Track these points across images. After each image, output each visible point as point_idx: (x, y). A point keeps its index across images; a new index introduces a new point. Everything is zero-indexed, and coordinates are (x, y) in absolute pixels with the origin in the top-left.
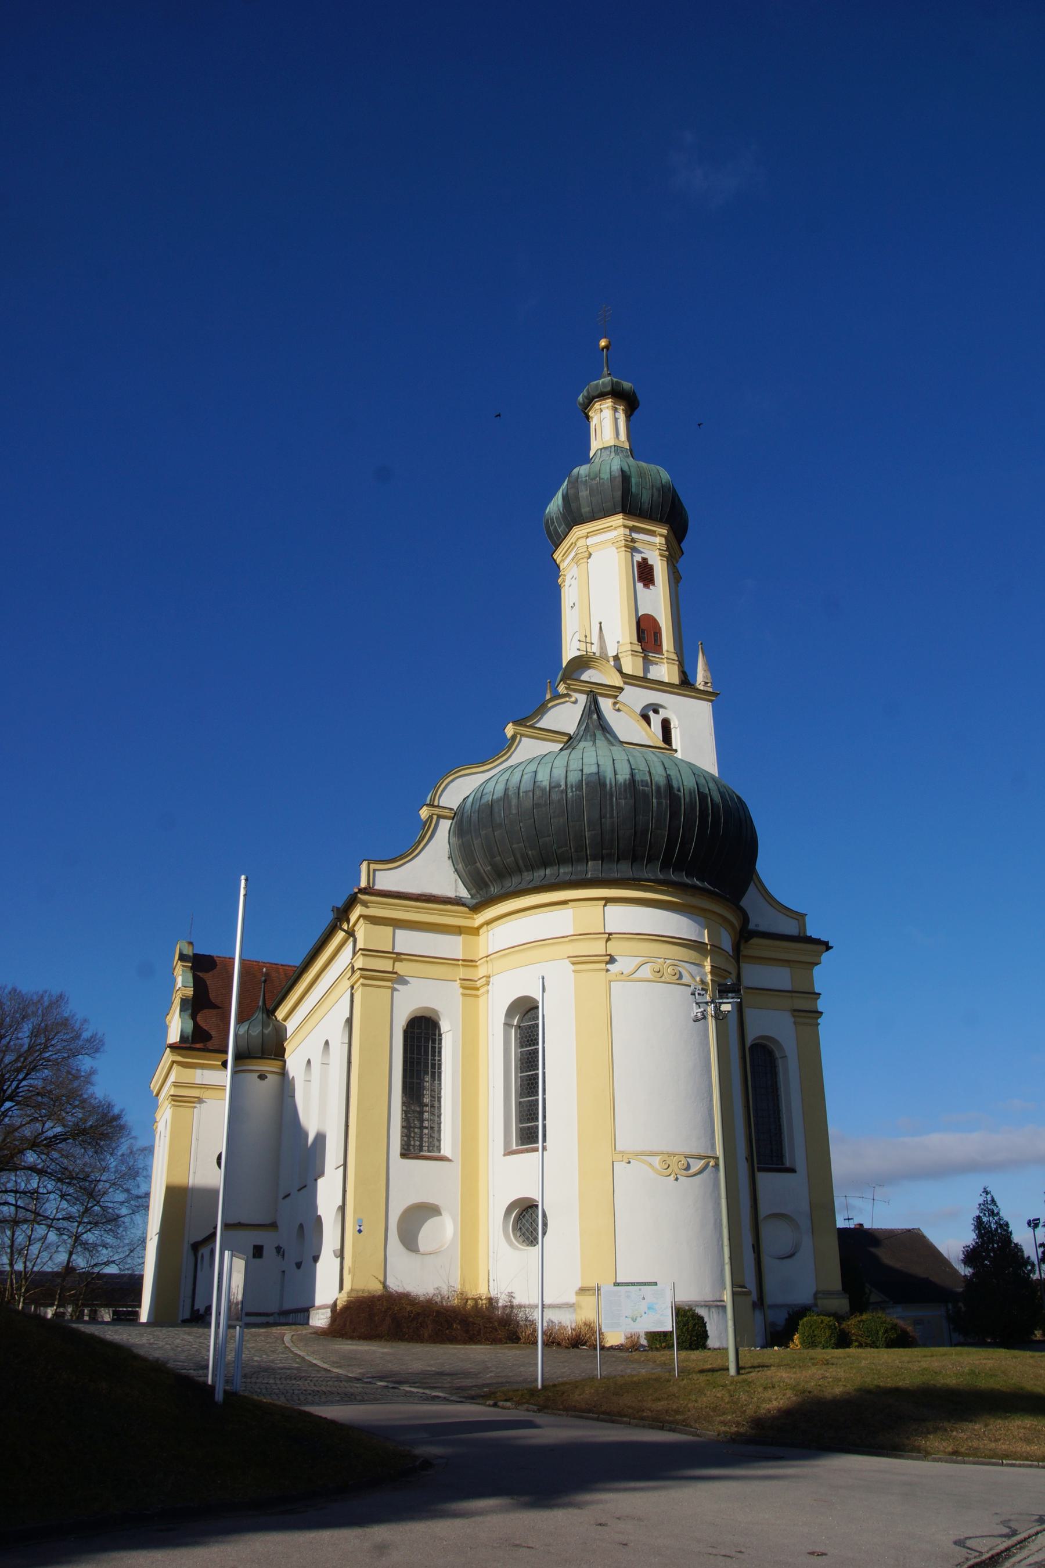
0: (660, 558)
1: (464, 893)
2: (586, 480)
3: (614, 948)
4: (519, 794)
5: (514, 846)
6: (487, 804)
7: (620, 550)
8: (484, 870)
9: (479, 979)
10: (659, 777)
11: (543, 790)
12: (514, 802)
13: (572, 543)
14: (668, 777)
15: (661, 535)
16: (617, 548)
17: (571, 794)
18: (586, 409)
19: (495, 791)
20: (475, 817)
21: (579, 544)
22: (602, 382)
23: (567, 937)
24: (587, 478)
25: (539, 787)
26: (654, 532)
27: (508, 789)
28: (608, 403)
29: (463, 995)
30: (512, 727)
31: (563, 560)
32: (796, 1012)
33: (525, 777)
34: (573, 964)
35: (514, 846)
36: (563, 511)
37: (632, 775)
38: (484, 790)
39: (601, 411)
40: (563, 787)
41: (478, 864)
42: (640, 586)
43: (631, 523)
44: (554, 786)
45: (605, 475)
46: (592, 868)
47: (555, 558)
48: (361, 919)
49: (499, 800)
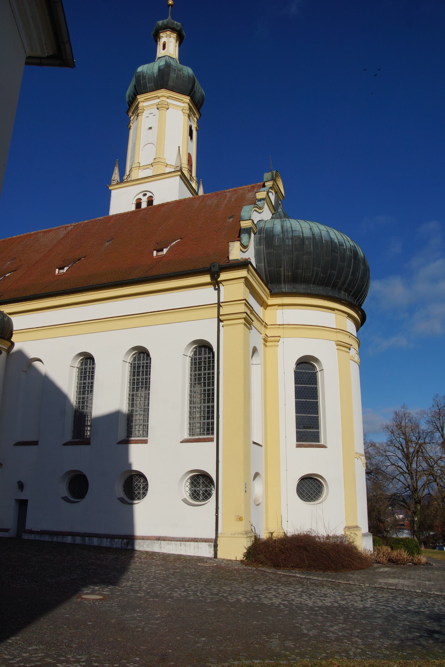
0: (195, 129)
2: (175, 69)
4: (322, 240)
5: (315, 268)
6: (299, 237)
7: (185, 114)
8: (285, 275)
9: (271, 337)
11: (336, 244)
13: (157, 96)
15: (197, 118)
16: (184, 113)
17: (348, 253)
18: (160, 30)
19: (304, 232)
20: (289, 242)
21: (162, 99)
22: (177, 24)
23: (336, 329)
24: (176, 68)
26: (196, 115)
27: (314, 234)
28: (174, 35)
30: (266, 194)
31: (143, 102)
34: (337, 345)
35: (315, 268)
36: (157, 76)
38: (293, 228)
39: (170, 37)
40: (345, 247)
43: (191, 105)
47: (138, 97)
48: (244, 279)
49: (308, 238)
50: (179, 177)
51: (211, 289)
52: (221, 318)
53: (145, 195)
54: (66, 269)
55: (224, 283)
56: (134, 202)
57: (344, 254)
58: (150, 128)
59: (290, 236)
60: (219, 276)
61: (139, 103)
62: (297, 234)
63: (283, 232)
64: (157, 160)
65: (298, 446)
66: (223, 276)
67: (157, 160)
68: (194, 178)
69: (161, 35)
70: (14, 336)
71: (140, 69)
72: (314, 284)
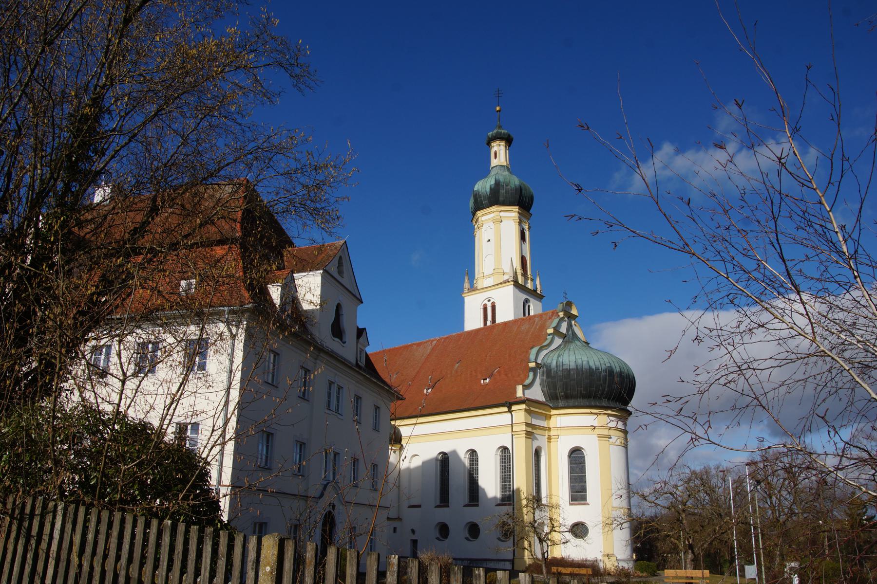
5: (579, 389)
6: (567, 369)
11: (593, 370)
20: (560, 373)
33: (584, 362)
41: (558, 391)
44: (597, 369)
45: (513, 186)
46: (604, 403)
49: (573, 369)
50: (512, 286)
51: (509, 414)
52: (513, 433)
53: (489, 301)
56: (482, 307)
57: (600, 376)
58: (489, 241)
59: (561, 369)
61: (478, 219)
62: (565, 367)
63: (557, 366)
64: (496, 271)
65: (571, 504)
66: (514, 408)
67: (496, 271)
68: (529, 276)
69: (493, 144)
70: (403, 440)
71: (476, 188)
72: (580, 398)
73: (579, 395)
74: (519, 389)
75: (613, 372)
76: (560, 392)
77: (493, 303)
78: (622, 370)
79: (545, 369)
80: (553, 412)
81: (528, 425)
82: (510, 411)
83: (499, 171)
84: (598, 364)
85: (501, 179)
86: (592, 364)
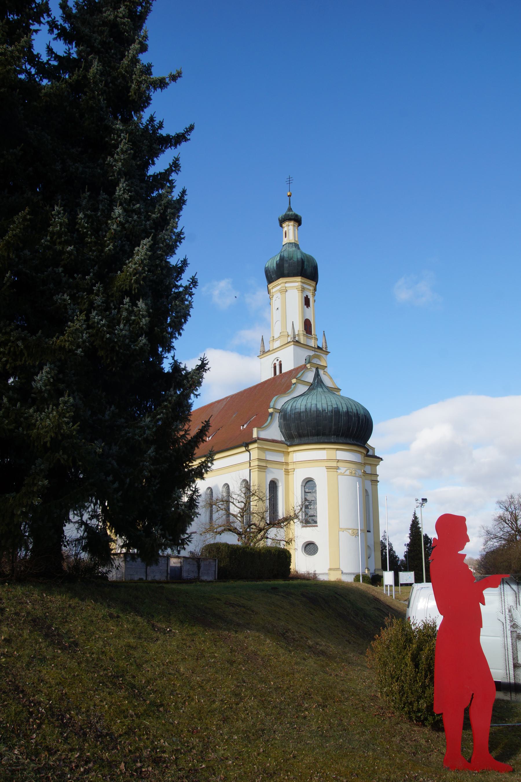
1: (283, 439)
3: (339, 464)
10: (355, 411)
11: (320, 411)
12: (309, 414)
14: (357, 410)
20: (293, 416)
25: (318, 410)
29: (285, 474)
31: (272, 289)
32: (372, 481)
33: (313, 405)
34: (327, 469)
37: (347, 409)
40: (327, 411)
41: (292, 431)
42: (306, 306)
43: (303, 281)
44: (324, 410)
45: (295, 260)
49: (303, 412)
50: (293, 346)
51: (248, 453)
52: (251, 468)
54: (210, 437)
55: (251, 450)
56: (273, 366)
58: (278, 309)
59: (294, 412)
60: (248, 447)
62: (297, 411)
66: (251, 447)
67: (282, 334)
69: (284, 225)
73: (309, 434)
74: (255, 430)
75: (339, 412)
76: (294, 432)
77: (280, 361)
78: (350, 410)
79: (283, 413)
80: (291, 449)
81: (259, 460)
82: (248, 451)
83: (287, 248)
84: (325, 406)
85: (286, 255)
86: (319, 406)
